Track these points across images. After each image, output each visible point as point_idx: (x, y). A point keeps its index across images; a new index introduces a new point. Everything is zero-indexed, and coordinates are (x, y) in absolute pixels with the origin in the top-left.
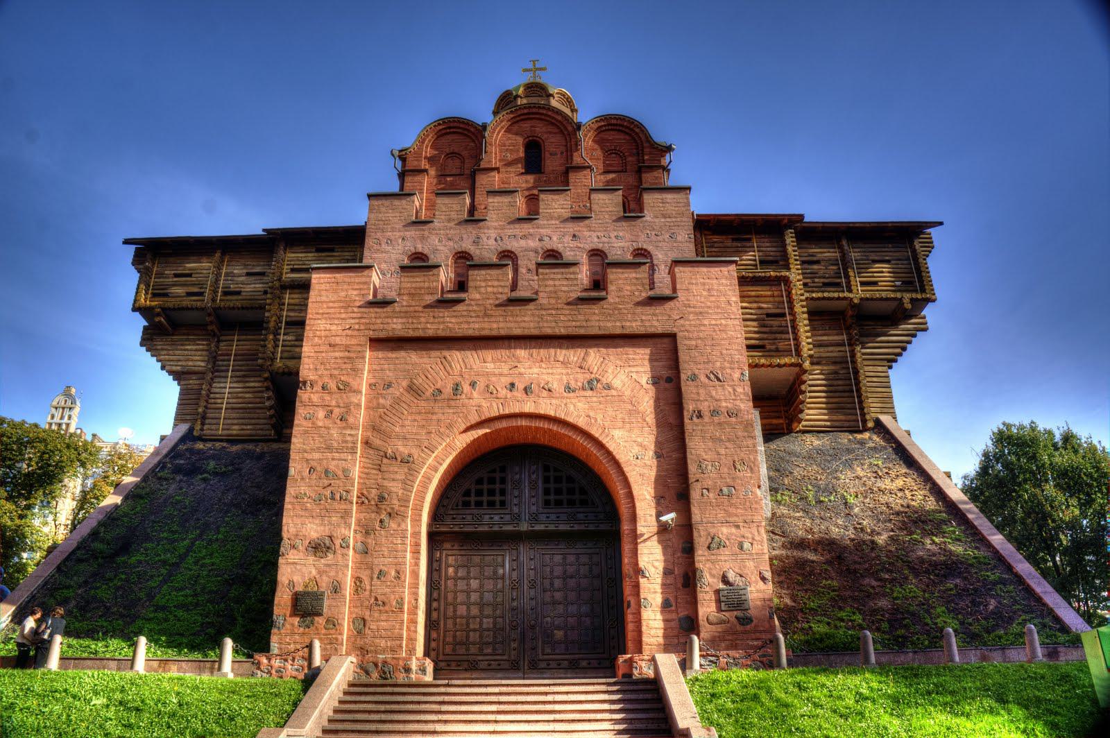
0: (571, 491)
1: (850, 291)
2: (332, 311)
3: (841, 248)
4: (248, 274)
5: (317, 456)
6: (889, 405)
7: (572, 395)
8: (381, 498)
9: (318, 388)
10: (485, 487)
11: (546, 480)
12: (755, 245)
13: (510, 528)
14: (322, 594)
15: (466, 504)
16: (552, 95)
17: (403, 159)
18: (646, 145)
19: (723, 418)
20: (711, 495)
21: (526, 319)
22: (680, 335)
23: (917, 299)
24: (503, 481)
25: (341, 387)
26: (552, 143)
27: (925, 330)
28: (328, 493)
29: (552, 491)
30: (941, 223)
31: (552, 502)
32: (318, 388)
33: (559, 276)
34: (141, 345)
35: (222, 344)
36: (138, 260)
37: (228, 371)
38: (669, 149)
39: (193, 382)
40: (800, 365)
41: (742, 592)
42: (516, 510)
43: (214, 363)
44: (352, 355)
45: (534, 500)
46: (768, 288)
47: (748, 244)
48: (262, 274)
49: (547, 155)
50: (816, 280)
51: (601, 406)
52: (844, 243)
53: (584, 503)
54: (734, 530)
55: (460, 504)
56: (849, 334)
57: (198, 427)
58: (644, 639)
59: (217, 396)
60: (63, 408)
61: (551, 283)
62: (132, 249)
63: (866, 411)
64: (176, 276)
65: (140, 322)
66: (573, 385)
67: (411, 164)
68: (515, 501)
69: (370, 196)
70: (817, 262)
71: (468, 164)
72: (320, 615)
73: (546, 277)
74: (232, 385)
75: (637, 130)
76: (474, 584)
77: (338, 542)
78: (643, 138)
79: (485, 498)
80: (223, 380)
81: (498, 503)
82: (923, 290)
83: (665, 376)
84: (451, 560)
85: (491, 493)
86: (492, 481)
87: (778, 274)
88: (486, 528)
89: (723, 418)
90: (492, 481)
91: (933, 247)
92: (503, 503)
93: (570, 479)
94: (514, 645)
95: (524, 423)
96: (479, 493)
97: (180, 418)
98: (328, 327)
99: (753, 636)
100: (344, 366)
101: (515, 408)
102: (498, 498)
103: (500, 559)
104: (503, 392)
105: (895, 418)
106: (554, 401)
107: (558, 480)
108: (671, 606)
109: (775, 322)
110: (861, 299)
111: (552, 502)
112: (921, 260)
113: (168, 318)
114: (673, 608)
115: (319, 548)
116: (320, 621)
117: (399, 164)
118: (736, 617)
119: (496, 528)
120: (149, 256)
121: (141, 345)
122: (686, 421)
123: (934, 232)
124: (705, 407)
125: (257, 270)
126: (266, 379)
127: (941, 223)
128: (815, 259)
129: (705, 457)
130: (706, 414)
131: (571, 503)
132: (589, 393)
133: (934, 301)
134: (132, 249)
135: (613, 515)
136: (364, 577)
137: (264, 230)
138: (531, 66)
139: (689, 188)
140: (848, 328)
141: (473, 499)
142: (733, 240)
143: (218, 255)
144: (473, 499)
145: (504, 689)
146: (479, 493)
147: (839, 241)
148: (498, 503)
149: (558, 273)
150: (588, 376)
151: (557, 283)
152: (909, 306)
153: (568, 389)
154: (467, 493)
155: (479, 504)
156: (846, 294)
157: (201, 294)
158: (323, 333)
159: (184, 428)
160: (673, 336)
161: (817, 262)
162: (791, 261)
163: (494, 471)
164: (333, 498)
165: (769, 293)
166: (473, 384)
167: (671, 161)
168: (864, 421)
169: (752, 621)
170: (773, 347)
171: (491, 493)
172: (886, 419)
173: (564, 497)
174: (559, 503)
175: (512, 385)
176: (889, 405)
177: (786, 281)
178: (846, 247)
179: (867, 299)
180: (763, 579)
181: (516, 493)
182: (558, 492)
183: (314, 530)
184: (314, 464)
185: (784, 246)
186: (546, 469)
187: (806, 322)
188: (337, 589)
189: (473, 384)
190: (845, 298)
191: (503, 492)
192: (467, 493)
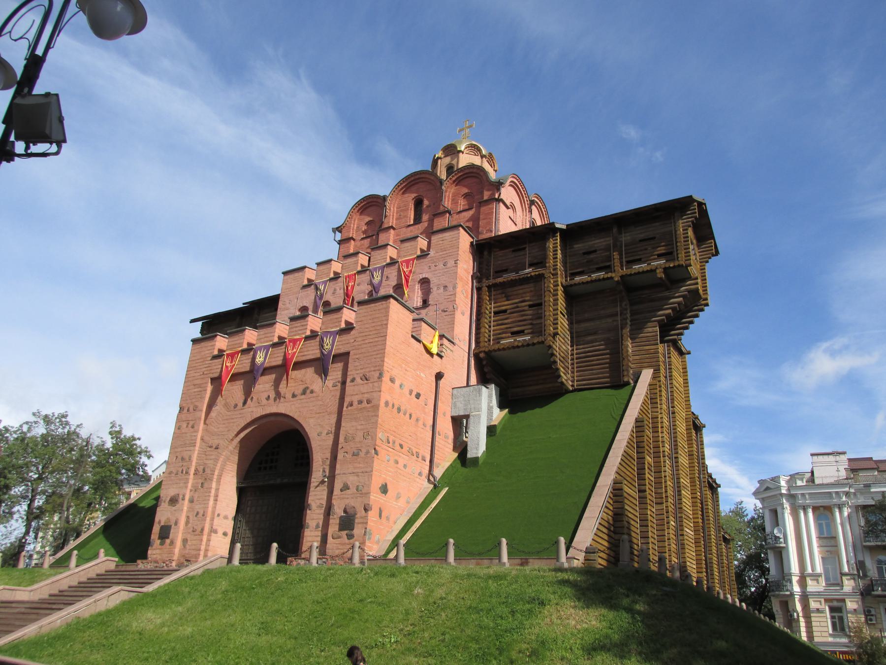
8: (204, 471)
15: (260, 469)
19: (365, 404)
47: (522, 253)
62: (200, 323)
69: (283, 273)
70: (595, 251)
72: (168, 538)
89: (365, 404)
104: (265, 402)
116: (168, 541)
124: (355, 400)
132: (303, 397)
134: (200, 323)
142: (514, 251)
150: (304, 386)
161: (595, 251)
184: (178, 454)
188: (176, 523)
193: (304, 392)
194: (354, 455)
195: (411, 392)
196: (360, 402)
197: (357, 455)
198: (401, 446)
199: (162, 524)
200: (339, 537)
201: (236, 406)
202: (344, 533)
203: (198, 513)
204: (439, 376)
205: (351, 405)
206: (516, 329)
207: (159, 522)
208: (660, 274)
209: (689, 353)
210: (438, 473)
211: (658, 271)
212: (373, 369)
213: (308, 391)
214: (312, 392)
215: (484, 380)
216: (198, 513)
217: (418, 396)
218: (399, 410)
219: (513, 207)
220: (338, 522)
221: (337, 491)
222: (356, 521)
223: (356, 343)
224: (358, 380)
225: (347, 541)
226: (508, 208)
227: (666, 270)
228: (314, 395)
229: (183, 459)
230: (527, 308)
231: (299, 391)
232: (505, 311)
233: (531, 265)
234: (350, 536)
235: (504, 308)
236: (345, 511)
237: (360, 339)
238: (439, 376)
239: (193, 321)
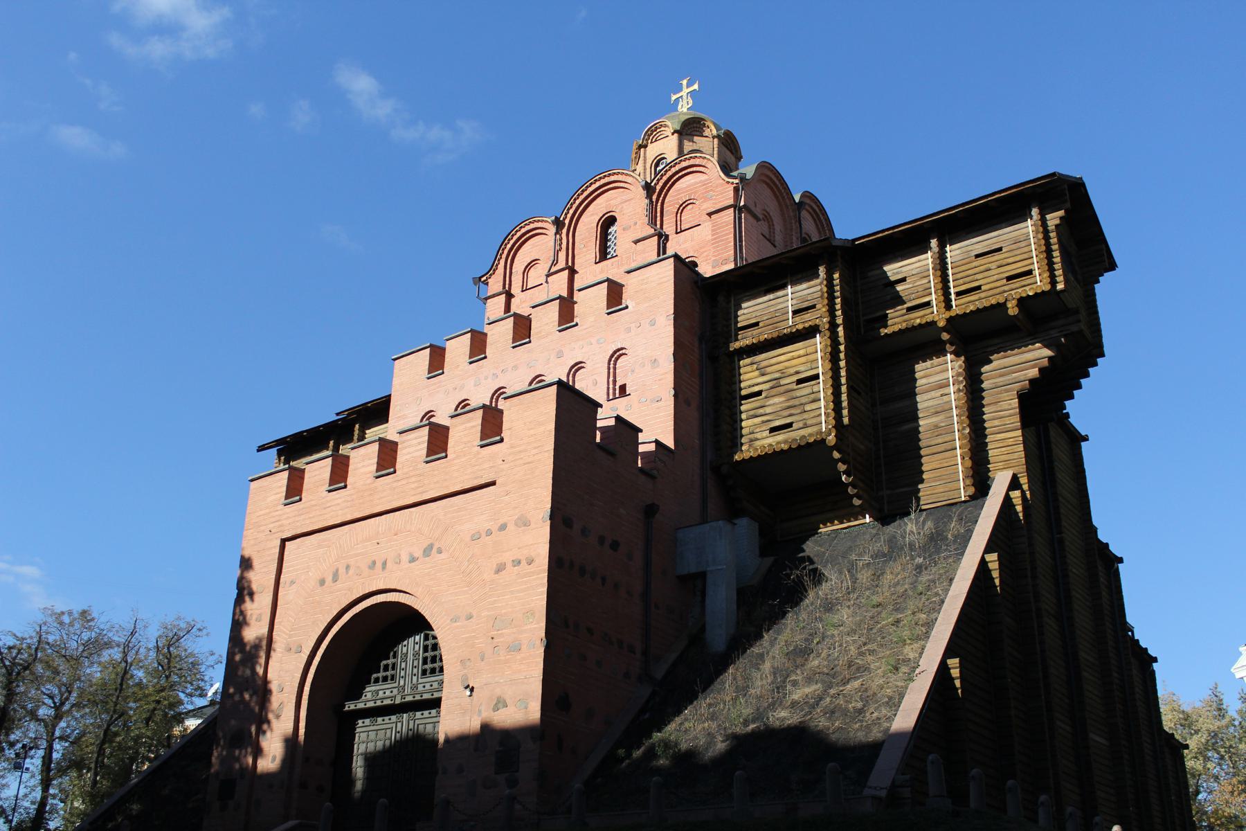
33: (415, 442)
45: (415, 671)
66: (416, 555)
109: (806, 389)
130: (509, 565)
152: (1013, 310)
156: (929, 318)
165: (802, 352)
166: (348, 567)
170: (801, 425)
175: (374, 563)
189: (348, 567)
193: (428, 551)
195: (602, 540)
198: (589, 630)
201: (322, 582)
204: (650, 511)
205: (500, 569)
206: (777, 423)
208: (1013, 310)
209: (1085, 439)
210: (659, 672)
211: (1009, 305)
213: (435, 550)
214: (440, 551)
215: (732, 512)
217: (615, 545)
218: (582, 571)
219: (767, 218)
223: (505, 466)
224: (511, 527)
226: (758, 219)
227: (1022, 302)
228: (443, 556)
231: (418, 553)
232: (759, 393)
234: (512, 783)
235: (756, 389)
238: (650, 511)
239: (262, 448)
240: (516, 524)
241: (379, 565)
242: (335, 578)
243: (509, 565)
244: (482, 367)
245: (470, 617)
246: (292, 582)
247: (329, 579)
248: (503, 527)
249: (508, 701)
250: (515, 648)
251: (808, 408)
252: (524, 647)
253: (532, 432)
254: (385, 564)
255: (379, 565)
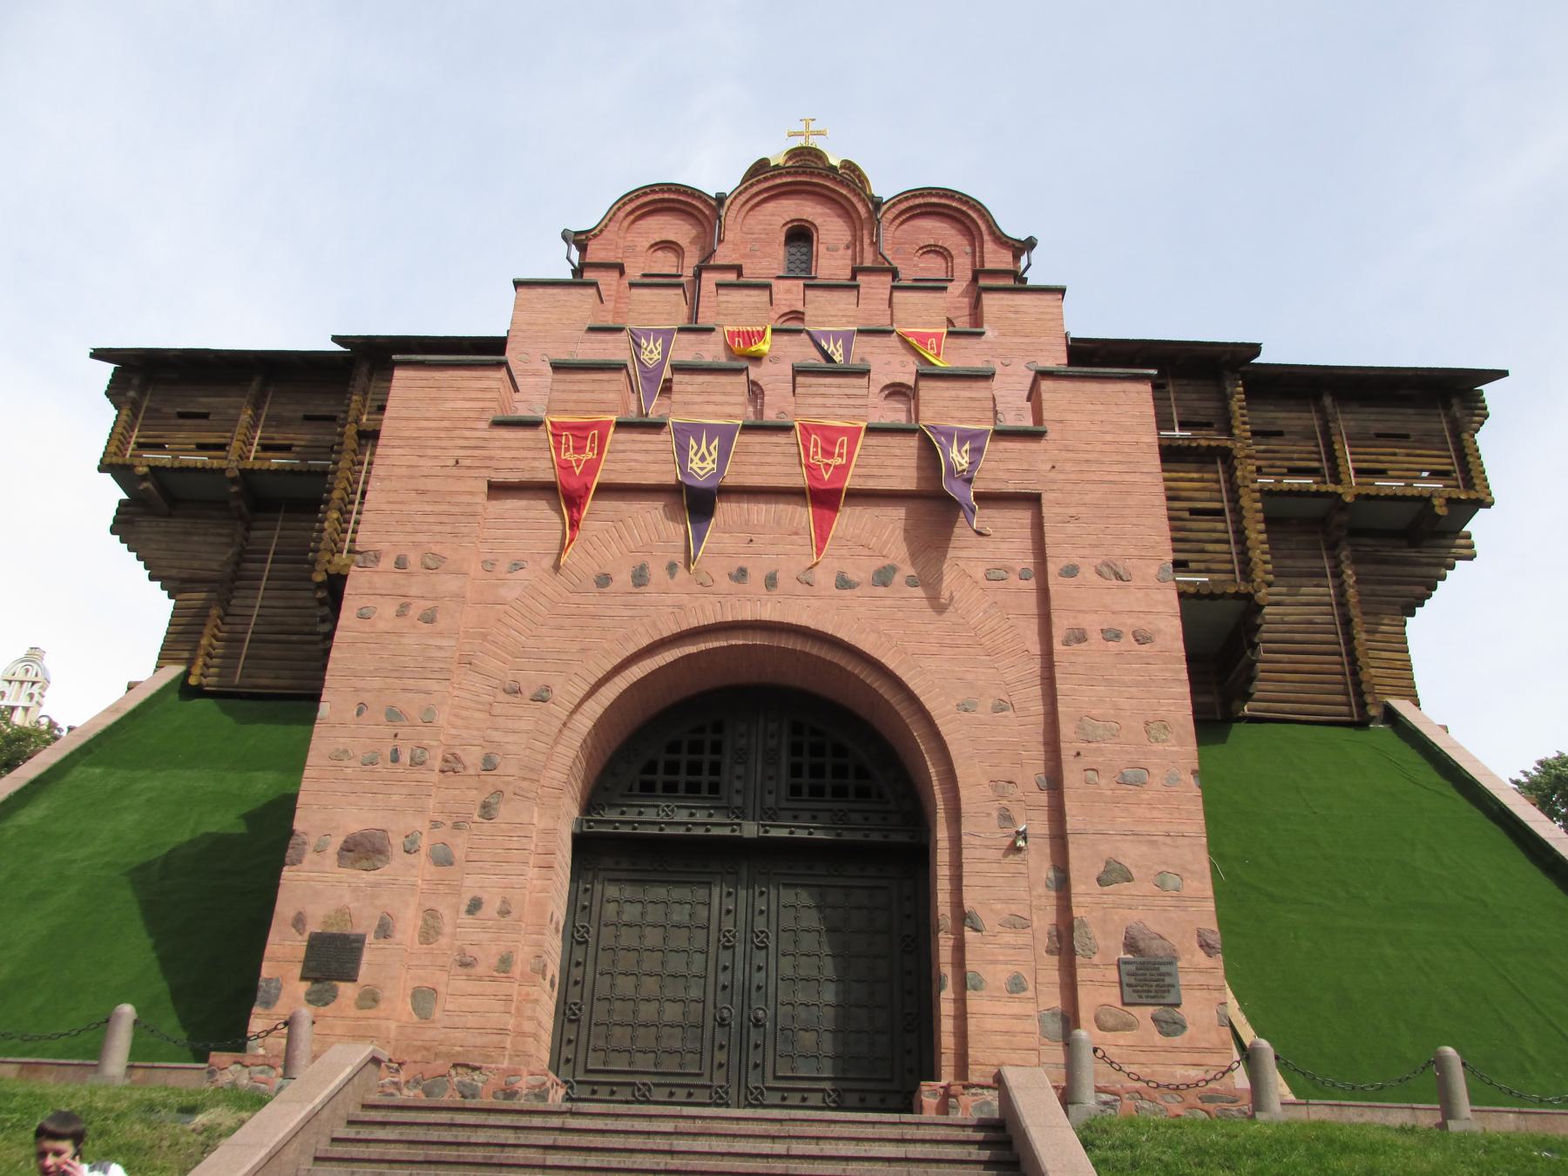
0: (840, 771)
1: (1338, 481)
2: (422, 434)
3: (1321, 411)
4: (307, 418)
5: (377, 683)
6: (1405, 683)
7: (848, 593)
8: (489, 765)
9: (387, 563)
10: (684, 758)
11: (796, 749)
12: (1172, 396)
13: (726, 832)
14: (360, 940)
15: (647, 788)
16: (833, 168)
17: (582, 248)
18: (986, 237)
19: (1127, 642)
20: (1103, 782)
21: (769, 459)
22: (1045, 498)
23: (1459, 501)
24: (717, 748)
25: (431, 564)
26: (831, 230)
27: (1471, 557)
28: (388, 752)
29: (806, 769)
30: (1504, 374)
31: (805, 790)
32: (387, 563)
33: (834, 391)
34: (113, 531)
35: (253, 534)
36: (115, 391)
37: (260, 579)
38: (1030, 244)
39: (197, 597)
40: (1249, 597)
41: (1163, 969)
42: (737, 801)
43: (237, 564)
44: (454, 509)
46: (1192, 466)
48: (333, 419)
49: (822, 248)
50: (1278, 463)
51: (900, 615)
52: (1328, 401)
53: (862, 793)
54: (1145, 849)
55: (637, 785)
56: (1331, 557)
57: (197, 670)
58: (970, 1052)
59: (237, 620)
60: (22, 682)
61: (819, 400)
62: (108, 369)
63: (1364, 687)
64: (182, 416)
65: (112, 493)
66: (852, 575)
67: (596, 253)
68: (738, 785)
69: (518, 284)
71: (692, 260)
72: (351, 977)
73: (812, 390)
74: (265, 603)
75: (974, 215)
76: (653, 937)
77: (397, 842)
78: (983, 227)
79: (683, 778)
80: (251, 592)
81: (705, 787)
82: (1469, 483)
83: (1019, 569)
84: (612, 891)
85: (695, 768)
86: (696, 748)
87: (1213, 443)
88: (681, 831)
90: (696, 748)
91: (1486, 416)
92: (714, 789)
93: (840, 750)
94: (721, 1057)
95: (758, 640)
96: (672, 768)
97: (165, 656)
98: (415, 461)
99: (1187, 1058)
100: (438, 528)
101: (747, 613)
102: (705, 778)
103: (701, 893)
104: (725, 584)
105: (1418, 705)
106: (815, 603)
107: (817, 750)
108: (1025, 989)
110: (1358, 496)
111: (805, 790)
112: (1465, 436)
113: (162, 487)
114: (1030, 994)
115: (363, 850)
116: (346, 990)
117: (575, 255)
118: (1154, 1019)
119: (700, 831)
120: (136, 381)
121: (113, 531)
122: (1058, 646)
123: (1489, 391)
125: (324, 411)
126: (320, 586)
127: (1504, 374)
128: (1275, 428)
129: (1094, 712)
130: (1095, 637)
131: (839, 793)
132: (881, 590)
133: (1489, 505)
134: (108, 369)
135: (917, 819)
136: (441, 910)
137: (336, 339)
138: (801, 127)
139: (1061, 291)
140: (1333, 547)
141: (660, 778)
143: (255, 385)
144: (660, 778)
145: (684, 1125)
146: (672, 768)
147: (1317, 398)
148: (705, 787)
149: (830, 386)
150: (880, 563)
151: (829, 401)
152: (1441, 511)
153: (843, 583)
154: (651, 768)
155: (670, 788)
156: (1331, 487)
157: (221, 447)
158: (404, 471)
159: (174, 671)
160: (1032, 500)
162: (1235, 423)
163: (701, 730)
164: (395, 758)
167: (1029, 265)
168: (1362, 706)
169: (1184, 1028)
170: (1202, 566)
171: (695, 768)
172: (1402, 706)
173: (828, 782)
174: (817, 792)
176: (1405, 683)
177: (1226, 456)
178: (1330, 410)
179: (1368, 497)
180: (1205, 946)
181: (739, 770)
182: (817, 771)
183: (355, 819)
184: (366, 697)
185: (1225, 399)
186: (797, 729)
187: (1262, 526)
188: (384, 931)
190: (1327, 494)
191: (715, 769)
192: (651, 768)
194: (1123, 781)
196: (1112, 635)
197: (1138, 783)
199: (314, 927)
200: (1128, 1026)
201: (604, 580)
202: (1143, 1014)
203: (475, 906)
205: (1080, 637)
207: (299, 922)
212: (1132, 551)
216: (475, 906)
220: (1113, 974)
221: (1083, 888)
222: (1183, 979)
223: (1053, 475)
224: (1087, 573)
225: (1159, 1040)
229: (393, 715)
230: (1186, 515)
233: (1184, 425)
234: (1171, 1026)
236: (1131, 945)
237: (1068, 467)
239: (99, 354)
240: (1100, 574)
241: (757, 577)
242: (640, 577)
243: (1095, 637)
244: (703, 342)
245: (1000, 707)
246: (517, 566)
247: (623, 578)
248: (1070, 571)
249: (1133, 871)
250: (1132, 780)
251: (1210, 547)
252: (1156, 782)
253: (1108, 437)
254: (771, 581)
255: (757, 577)
